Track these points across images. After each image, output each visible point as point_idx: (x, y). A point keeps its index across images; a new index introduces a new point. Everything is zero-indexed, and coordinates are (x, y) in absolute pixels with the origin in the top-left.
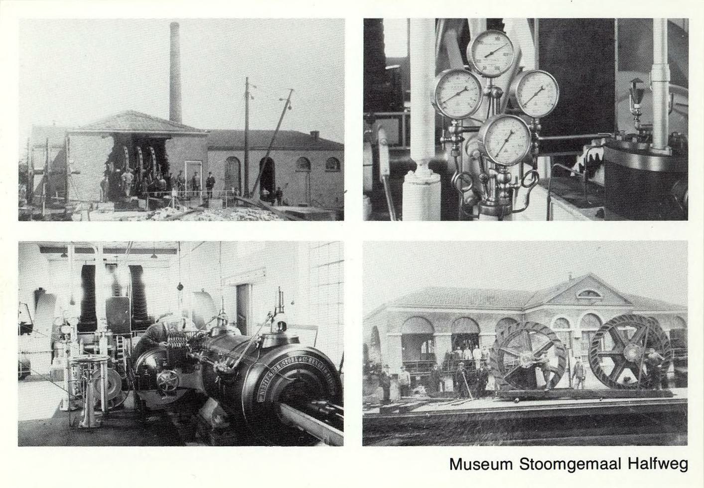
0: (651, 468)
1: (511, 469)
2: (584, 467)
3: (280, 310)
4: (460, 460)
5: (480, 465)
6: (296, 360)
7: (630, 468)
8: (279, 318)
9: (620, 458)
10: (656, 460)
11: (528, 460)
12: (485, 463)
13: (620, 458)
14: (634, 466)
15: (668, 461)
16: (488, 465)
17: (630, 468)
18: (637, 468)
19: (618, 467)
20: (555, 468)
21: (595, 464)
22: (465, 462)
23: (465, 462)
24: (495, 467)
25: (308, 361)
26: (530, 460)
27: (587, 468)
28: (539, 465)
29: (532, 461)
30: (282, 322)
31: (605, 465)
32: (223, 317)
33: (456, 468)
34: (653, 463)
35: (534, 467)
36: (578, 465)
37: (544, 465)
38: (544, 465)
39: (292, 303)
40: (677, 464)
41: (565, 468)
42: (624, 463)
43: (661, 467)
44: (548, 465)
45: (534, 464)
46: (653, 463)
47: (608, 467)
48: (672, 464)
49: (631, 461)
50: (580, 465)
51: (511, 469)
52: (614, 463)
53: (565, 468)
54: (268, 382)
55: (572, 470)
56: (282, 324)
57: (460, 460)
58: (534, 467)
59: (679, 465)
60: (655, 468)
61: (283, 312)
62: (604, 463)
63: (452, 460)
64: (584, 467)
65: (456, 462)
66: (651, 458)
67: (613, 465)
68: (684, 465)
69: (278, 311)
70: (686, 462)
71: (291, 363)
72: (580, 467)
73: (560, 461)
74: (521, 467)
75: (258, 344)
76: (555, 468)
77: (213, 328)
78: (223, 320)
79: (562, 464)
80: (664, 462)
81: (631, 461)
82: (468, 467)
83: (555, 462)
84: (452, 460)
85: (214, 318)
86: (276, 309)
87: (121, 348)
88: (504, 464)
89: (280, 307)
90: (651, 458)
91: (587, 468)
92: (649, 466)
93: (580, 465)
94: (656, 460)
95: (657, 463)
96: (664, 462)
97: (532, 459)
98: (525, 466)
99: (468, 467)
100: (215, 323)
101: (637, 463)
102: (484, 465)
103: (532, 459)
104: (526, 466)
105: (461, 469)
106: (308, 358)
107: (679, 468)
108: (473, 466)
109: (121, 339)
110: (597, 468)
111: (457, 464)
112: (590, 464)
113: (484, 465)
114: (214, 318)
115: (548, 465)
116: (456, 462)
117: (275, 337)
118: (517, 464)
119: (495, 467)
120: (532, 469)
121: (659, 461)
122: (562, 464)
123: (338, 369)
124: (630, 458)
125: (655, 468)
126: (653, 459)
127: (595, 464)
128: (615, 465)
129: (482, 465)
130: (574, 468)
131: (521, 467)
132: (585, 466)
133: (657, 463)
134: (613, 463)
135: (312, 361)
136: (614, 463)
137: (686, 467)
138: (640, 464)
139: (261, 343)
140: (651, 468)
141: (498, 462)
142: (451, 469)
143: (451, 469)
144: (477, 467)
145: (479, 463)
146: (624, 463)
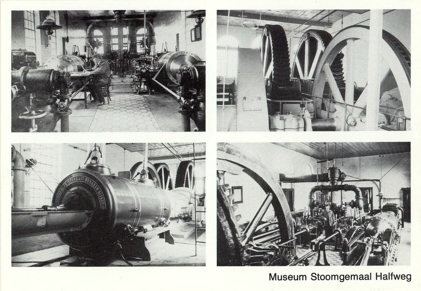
0: (389, 279)
1: (306, 280)
2: (349, 279)
4: (275, 274)
5: (287, 277)
7: (377, 279)
9: (371, 273)
10: (393, 274)
11: (316, 274)
12: (347, 276)
13: (371, 273)
14: (379, 278)
15: (400, 275)
16: (292, 277)
17: (377, 279)
18: (381, 279)
19: (369, 278)
20: (332, 279)
21: (356, 277)
22: (278, 276)
23: (278, 276)
24: (296, 278)
26: (317, 274)
27: (351, 279)
28: (323, 278)
29: (318, 275)
31: (362, 277)
33: (273, 279)
34: (390, 276)
35: (319, 279)
36: (346, 277)
37: (325, 278)
38: (325, 278)
40: (405, 277)
41: (338, 279)
42: (373, 276)
43: (395, 279)
44: (328, 278)
45: (319, 277)
46: (390, 276)
47: (364, 278)
48: (402, 277)
49: (378, 275)
50: (346, 277)
51: (306, 280)
52: (386, 276)
53: (338, 279)
55: (342, 281)
57: (275, 274)
58: (319, 279)
59: (406, 278)
60: (392, 279)
62: (361, 276)
63: (270, 274)
64: (349, 279)
65: (273, 276)
66: (389, 273)
67: (385, 277)
68: (409, 277)
70: (410, 275)
72: (347, 278)
73: (355, 275)
74: (312, 278)
76: (332, 279)
79: (336, 277)
80: (397, 275)
81: (378, 275)
82: (280, 278)
83: (351, 276)
84: (270, 274)
88: (301, 277)
90: (389, 273)
91: (351, 279)
92: (388, 278)
93: (346, 277)
94: (393, 274)
95: (393, 276)
96: (397, 275)
97: (318, 274)
98: (314, 278)
99: (280, 278)
101: (381, 276)
102: (290, 277)
103: (318, 274)
104: (314, 278)
105: (276, 280)
107: (406, 279)
108: (283, 278)
110: (357, 279)
111: (273, 277)
112: (353, 277)
113: (290, 277)
115: (328, 278)
116: (273, 276)
118: (309, 277)
119: (296, 278)
120: (319, 280)
121: (394, 275)
122: (336, 277)
124: (376, 273)
125: (392, 279)
126: (390, 274)
127: (356, 277)
128: (368, 277)
129: (289, 278)
130: (343, 279)
131: (312, 278)
132: (350, 278)
133: (393, 276)
134: (367, 276)
136: (386, 276)
137: (410, 279)
138: (382, 277)
140: (389, 279)
141: (298, 276)
142: (270, 280)
143: (270, 280)
144: (285, 279)
145: (286, 276)
146: (373, 276)
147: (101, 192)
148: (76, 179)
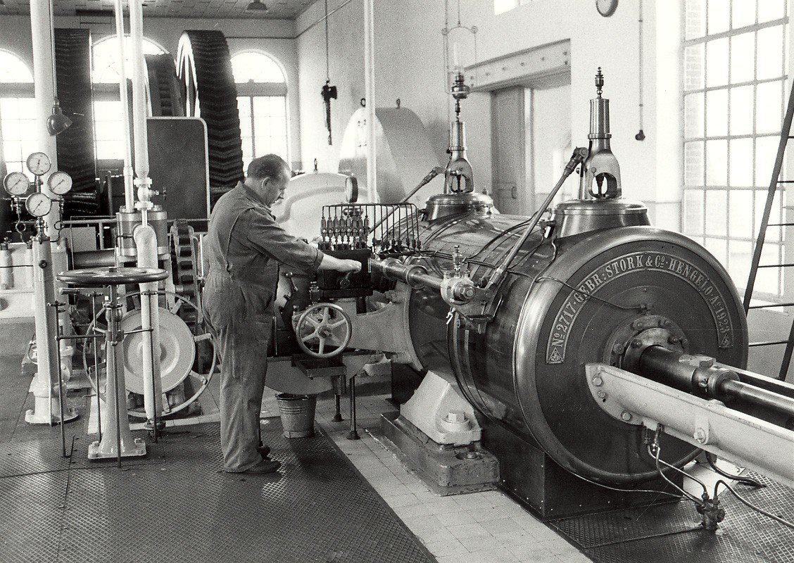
3: (601, 144)
6: (639, 262)
8: (600, 163)
25: (666, 267)
30: (606, 174)
32: (461, 170)
39: (640, 136)
54: (571, 316)
56: (605, 180)
61: (608, 151)
69: (596, 146)
71: (627, 270)
75: (548, 229)
77: (432, 199)
78: (459, 177)
85: (434, 173)
86: (591, 143)
87: (186, 259)
89: (601, 138)
100: (438, 186)
106: (668, 259)
109: (187, 233)
114: (434, 173)
117: (589, 212)
123: (740, 285)
135: (676, 267)
139: (555, 226)
147: (719, 299)
148: (635, 262)
